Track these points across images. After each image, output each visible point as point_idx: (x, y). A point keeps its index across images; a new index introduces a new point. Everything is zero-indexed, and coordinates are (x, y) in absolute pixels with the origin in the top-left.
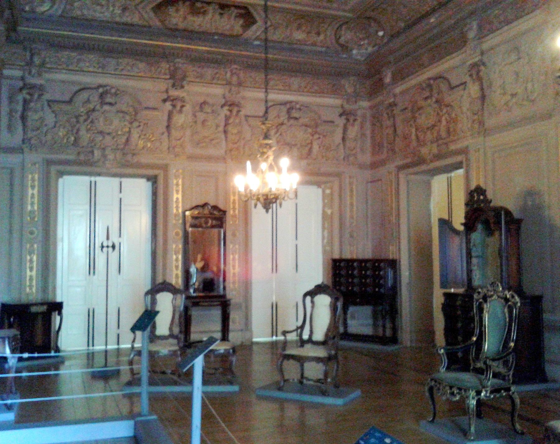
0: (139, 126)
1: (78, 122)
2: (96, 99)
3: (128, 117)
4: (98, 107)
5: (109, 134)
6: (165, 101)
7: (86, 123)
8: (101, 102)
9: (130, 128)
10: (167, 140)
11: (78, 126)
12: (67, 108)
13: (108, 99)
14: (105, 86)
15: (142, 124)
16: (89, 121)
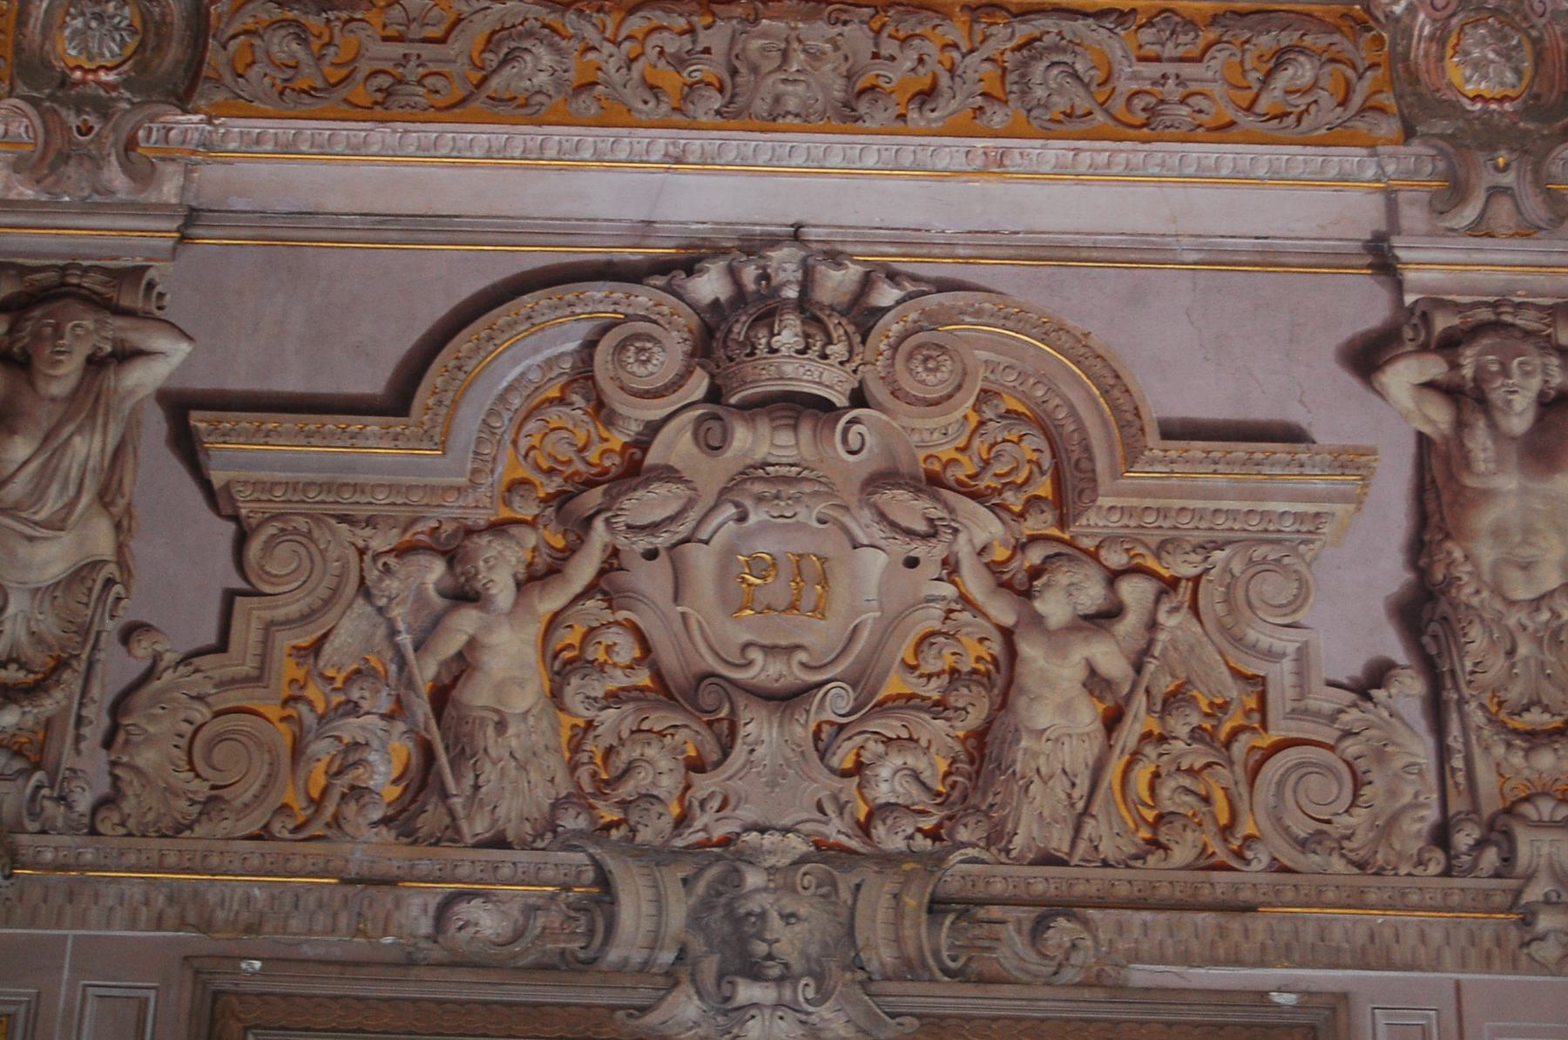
0: (1111, 614)
1: (464, 595)
2: (668, 357)
3: (983, 527)
4: (676, 445)
5: (785, 699)
6: (1366, 357)
7: (550, 601)
8: (715, 395)
9: (1007, 634)
10: (1422, 750)
11: (467, 621)
12: (376, 450)
13: (790, 361)
14: (754, 245)
15: (1134, 592)
16: (584, 570)
